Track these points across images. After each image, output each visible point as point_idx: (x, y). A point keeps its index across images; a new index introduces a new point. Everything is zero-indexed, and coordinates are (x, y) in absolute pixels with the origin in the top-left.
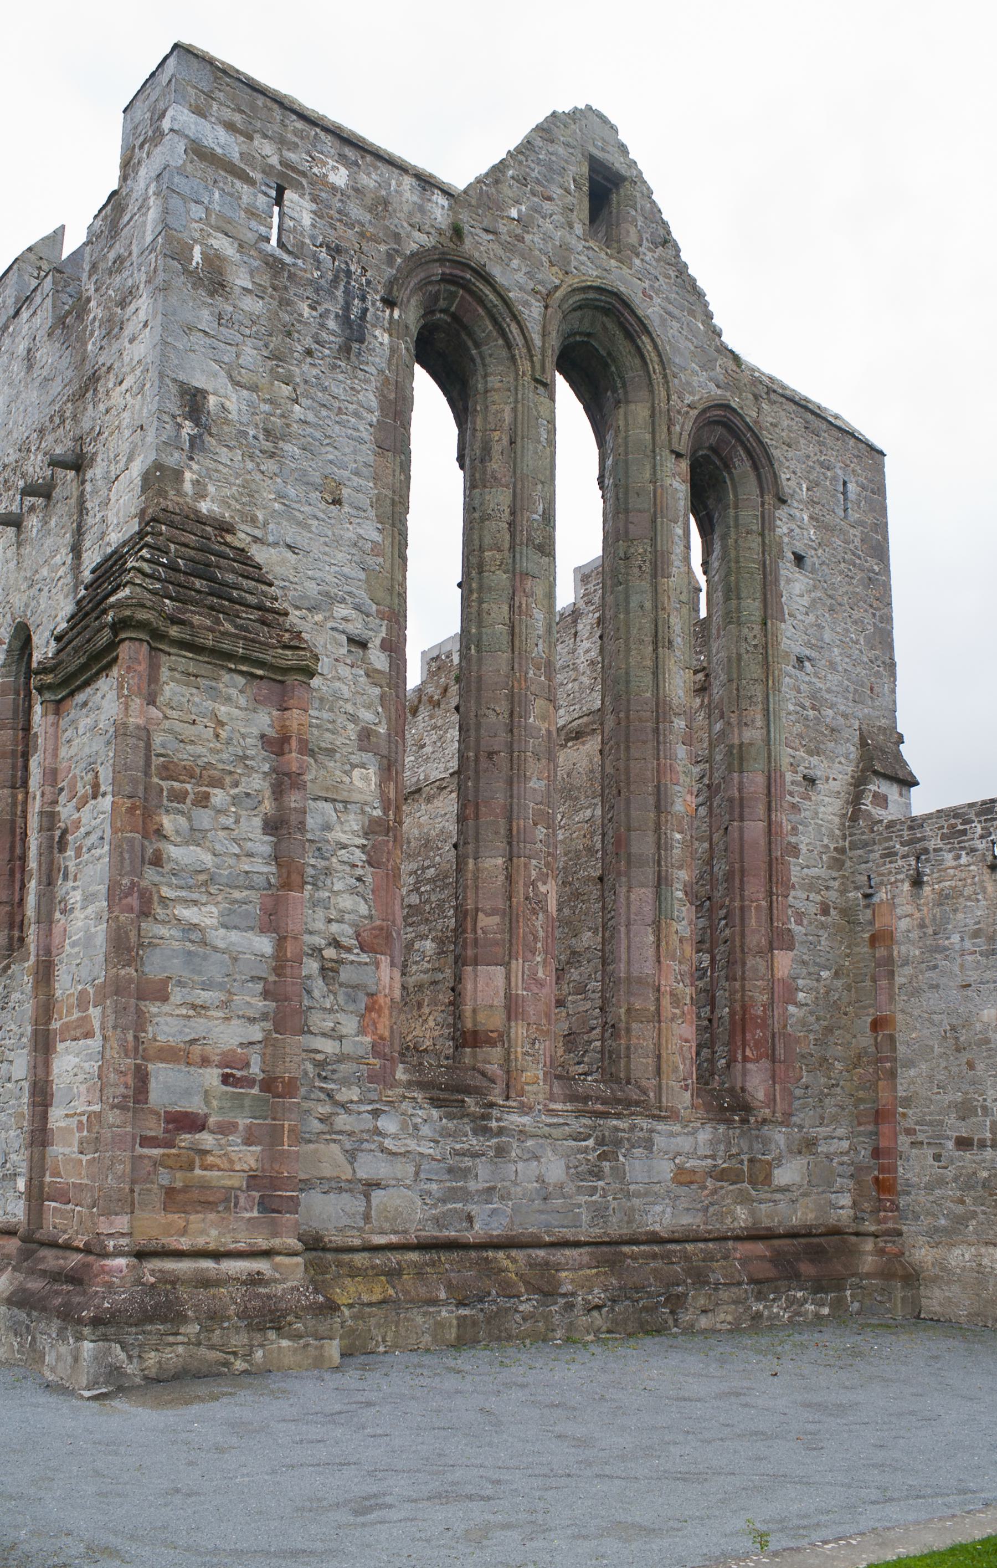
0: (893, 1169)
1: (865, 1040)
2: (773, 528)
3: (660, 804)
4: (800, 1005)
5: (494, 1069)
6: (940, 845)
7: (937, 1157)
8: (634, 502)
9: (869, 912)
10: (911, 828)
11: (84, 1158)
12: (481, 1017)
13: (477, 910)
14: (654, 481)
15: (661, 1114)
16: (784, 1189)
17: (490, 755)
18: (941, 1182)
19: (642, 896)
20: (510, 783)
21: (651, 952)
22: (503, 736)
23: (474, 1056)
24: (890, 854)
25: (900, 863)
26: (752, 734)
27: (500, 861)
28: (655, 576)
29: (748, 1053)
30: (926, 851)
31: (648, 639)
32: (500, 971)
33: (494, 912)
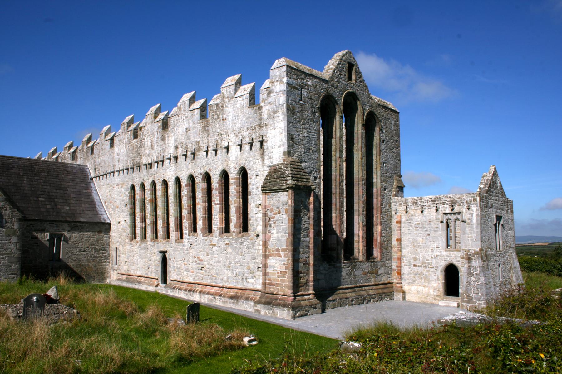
5: (335, 255)
6: (411, 204)
9: (396, 216)
11: (279, 279)
18: (410, 273)
25: (403, 207)
30: (408, 205)
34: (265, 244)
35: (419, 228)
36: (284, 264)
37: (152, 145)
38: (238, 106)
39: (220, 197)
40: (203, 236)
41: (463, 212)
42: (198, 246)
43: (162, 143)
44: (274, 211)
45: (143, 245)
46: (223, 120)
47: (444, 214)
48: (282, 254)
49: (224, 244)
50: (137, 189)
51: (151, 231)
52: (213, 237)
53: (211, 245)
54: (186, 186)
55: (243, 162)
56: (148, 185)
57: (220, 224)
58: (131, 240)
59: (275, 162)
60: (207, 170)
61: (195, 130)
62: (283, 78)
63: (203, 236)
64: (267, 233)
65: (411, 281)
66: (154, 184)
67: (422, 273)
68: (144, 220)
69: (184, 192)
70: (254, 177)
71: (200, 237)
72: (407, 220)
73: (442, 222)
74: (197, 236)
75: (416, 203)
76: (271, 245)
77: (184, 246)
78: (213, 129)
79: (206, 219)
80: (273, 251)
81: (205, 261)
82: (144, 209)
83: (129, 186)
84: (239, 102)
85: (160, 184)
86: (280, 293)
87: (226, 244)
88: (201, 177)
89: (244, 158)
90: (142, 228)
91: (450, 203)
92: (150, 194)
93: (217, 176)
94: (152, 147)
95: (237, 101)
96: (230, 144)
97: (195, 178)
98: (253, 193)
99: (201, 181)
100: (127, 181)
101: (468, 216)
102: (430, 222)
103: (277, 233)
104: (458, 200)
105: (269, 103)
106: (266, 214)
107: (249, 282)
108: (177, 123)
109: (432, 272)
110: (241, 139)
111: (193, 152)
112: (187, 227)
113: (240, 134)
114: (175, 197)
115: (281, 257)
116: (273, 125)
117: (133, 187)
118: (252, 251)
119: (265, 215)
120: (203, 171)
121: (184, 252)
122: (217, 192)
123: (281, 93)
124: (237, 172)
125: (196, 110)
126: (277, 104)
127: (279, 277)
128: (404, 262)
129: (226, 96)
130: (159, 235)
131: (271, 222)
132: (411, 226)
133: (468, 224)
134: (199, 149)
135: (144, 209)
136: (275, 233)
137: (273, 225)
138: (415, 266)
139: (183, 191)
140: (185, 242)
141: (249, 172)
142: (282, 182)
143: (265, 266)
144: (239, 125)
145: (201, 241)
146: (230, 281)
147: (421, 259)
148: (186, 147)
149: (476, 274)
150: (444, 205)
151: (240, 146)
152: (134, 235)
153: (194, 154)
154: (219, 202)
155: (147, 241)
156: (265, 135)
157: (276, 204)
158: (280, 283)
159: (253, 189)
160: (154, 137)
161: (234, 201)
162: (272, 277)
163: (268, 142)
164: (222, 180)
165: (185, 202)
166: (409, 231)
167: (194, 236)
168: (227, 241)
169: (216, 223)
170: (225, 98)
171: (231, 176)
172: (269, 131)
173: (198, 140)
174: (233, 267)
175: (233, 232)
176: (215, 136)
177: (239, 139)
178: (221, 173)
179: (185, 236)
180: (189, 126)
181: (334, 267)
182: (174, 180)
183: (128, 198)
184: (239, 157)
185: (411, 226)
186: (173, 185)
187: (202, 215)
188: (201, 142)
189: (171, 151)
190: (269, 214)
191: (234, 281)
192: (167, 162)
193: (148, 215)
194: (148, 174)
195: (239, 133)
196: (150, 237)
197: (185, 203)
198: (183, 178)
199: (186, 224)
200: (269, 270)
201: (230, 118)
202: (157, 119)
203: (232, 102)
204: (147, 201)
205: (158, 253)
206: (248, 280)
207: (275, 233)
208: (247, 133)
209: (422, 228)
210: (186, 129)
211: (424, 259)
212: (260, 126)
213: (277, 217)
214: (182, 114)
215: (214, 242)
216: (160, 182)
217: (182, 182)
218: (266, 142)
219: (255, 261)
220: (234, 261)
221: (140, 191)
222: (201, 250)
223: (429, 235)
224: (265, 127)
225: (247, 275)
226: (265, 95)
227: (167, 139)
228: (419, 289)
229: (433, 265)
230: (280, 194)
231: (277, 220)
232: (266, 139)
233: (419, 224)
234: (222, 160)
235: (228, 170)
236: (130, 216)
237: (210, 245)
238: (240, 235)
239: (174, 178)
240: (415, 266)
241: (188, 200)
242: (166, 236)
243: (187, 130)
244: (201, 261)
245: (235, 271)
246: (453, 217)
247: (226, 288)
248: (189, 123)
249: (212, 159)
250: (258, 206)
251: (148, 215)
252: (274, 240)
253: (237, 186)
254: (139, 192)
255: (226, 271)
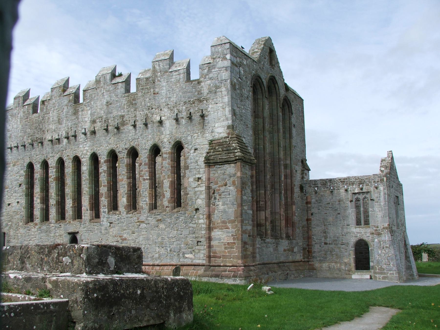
0: (311, 248)
1: (305, 223)
2: (291, 120)
3: (280, 179)
4: (296, 216)
7: (320, 246)
8: (274, 118)
10: (315, 182)
11: (226, 251)
12: (261, 221)
13: (260, 201)
14: (277, 113)
15: (282, 238)
16: (295, 253)
17: (261, 171)
19: (277, 195)
20: (265, 176)
21: (279, 207)
22: (263, 168)
23: (260, 228)
24: (310, 186)
25: (312, 188)
26: (288, 162)
27: (263, 192)
28: (278, 133)
29: (289, 226)
31: (277, 146)
32: (264, 212)
33: (262, 201)
34: (209, 217)
35: (329, 208)
36: (232, 235)
37: (59, 119)
38: (173, 80)
39: (150, 172)
40: (127, 214)
41: (371, 192)
42: (120, 225)
43: (74, 117)
44: (220, 184)
45: (44, 227)
46: (154, 94)
47: (353, 193)
48: (229, 225)
49: (154, 220)
50: (37, 167)
51: (56, 211)
52: (140, 213)
53: (138, 222)
54: (105, 162)
55: (179, 136)
56: (52, 163)
57: (150, 200)
58: (27, 223)
59: (217, 136)
60: (133, 144)
61: (118, 104)
62: (226, 54)
63: (127, 214)
64: (211, 205)
65: (322, 259)
66: (61, 162)
67: (333, 249)
68: (45, 200)
69: (102, 168)
70: (192, 151)
71: (124, 214)
72: (317, 201)
73: (351, 201)
74: (120, 214)
75: (326, 184)
76: (217, 218)
77: (101, 225)
78: (141, 103)
79: (130, 196)
80: (217, 223)
81: (129, 240)
82: (45, 189)
83: (26, 164)
84: (174, 77)
85: (71, 161)
86: (228, 264)
87: (158, 220)
88: (126, 152)
89: (180, 132)
90: (42, 209)
91: (358, 184)
92: (56, 172)
93: (146, 151)
94: (59, 122)
95: (172, 76)
96: (163, 118)
97: (118, 154)
98: (191, 167)
99: (125, 156)
100: (23, 159)
101: (376, 195)
102: (339, 201)
103: (223, 205)
104: (366, 180)
105: (210, 79)
106: (209, 187)
107: (186, 258)
108: (95, 97)
109: (343, 248)
110: (176, 112)
111: (116, 126)
112: (106, 204)
113: (176, 109)
114: (90, 174)
115: (228, 228)
116: (215, 100)
117: (31, 166)
118: (191, 225)
119: (209, 188)
120: (128, 146)
121: (101, 232)
122: (147, 166)
123: (225, 68)
124: (171, 146)
125: (120, 84)
126: (220, 80)
127: (226, 248)
128: (314, 241)
129: (159, 71)
130: (67, 215)
131: (215, 195)
132: (321, 206)
133: (376, 202)
134: (124, 123)
135: (45, 189)
136: (221, 205)
137: (218, 197)
138: (326, 244)
139: (102, 167)
140: (103, 221)
141: (185, 146)
142: (229, 154)
143: (210, 239)
144: (174, 99)
145: (124, 219)
146: (162, 259)
147: (332, 237)
148: (107, 121)
149: (387, 247)
150: (353, 185)
151: (177, 120)
152: (30, 218)
153: (118, 128)
154: (148, 178)
155: (51, 223)
156: (206, 110)
157: (222, 177)
158: (228, 254)
159: (191, 163)
160: (62, 111)
161: (168, 176)
162: (218, 249)
163: (209, 117)
164: (152, 155)
165: (104, 178)
166: (319, 211)
167: (115, 214)
168: (159, 217)
169: (144, 199)
170: (158, 72)
171: (163, 150)
172: (210, 106)
173: (123, 114)
174: (166, 244)
175: (167, 207)
176: (145, 110)
177: (174, 113)
178: (151, 147)
179: (102, 215)
180: (111, 100)
181: (265, 243)
182: (89, 156)
183: (23, 177)
184: (174, 131)
185: (321, 206)
186: (88, 162)
187: (126, 192)
188: (126, 116)
189: (88, 126)
190: (213, 186)
191: (168, 257)
192: (81, 137)
193: (53, 194)
194: (54, 150)
195: (174, 107)
196: (55, 218)
197: (104, 180)
198: (102, 154)
199: (104, 201)
200: (213, 243)
201: (163, 92)
202: (66, 93)
203: (165, 76)
204: (50, 180)
205: (67, 235)
206: (187, 256)
207: (220, 206)
208: (184, 108)
209: (332, 207)
210: (107, 103)
211: (334, 237)
212: (200, 101)
213: (222, 189)
214: (102, 87)
215: (143, 218)
216: (69, 159)
217: (101, 158)
218: (207, 116)
219: (194, 235)
220: (168, 238)
221: (41, 169)
222: (125, 228)
223: (339, 214)
224: (205, 102)
225: (184, 250)
226: (206, 70)
227: (80, 113)
228: (330, 266)
229: (343, 242)
230: (227, 166)
231: (223, 192)
232: (207, 113)
233: (329, 203)
234: (154, 134)
235: (160, 145)
236: (26, 196)
237: (136, 223)
238: (176, 210)
239: (89, 154)
240: (326, 244)
241: (107, 176)
242: (76, 217)
243: (108, 104)
244: (125, 239)
245: (169, 247)
246: (361, 197)
247: (158, 265)
248: (111, 97)
249: (140, 134)
250: (197, 179)
251: (53, 194)
252: (219, 212)
253: (171, 161)
254: (39, 170)
255: (157, 248)
